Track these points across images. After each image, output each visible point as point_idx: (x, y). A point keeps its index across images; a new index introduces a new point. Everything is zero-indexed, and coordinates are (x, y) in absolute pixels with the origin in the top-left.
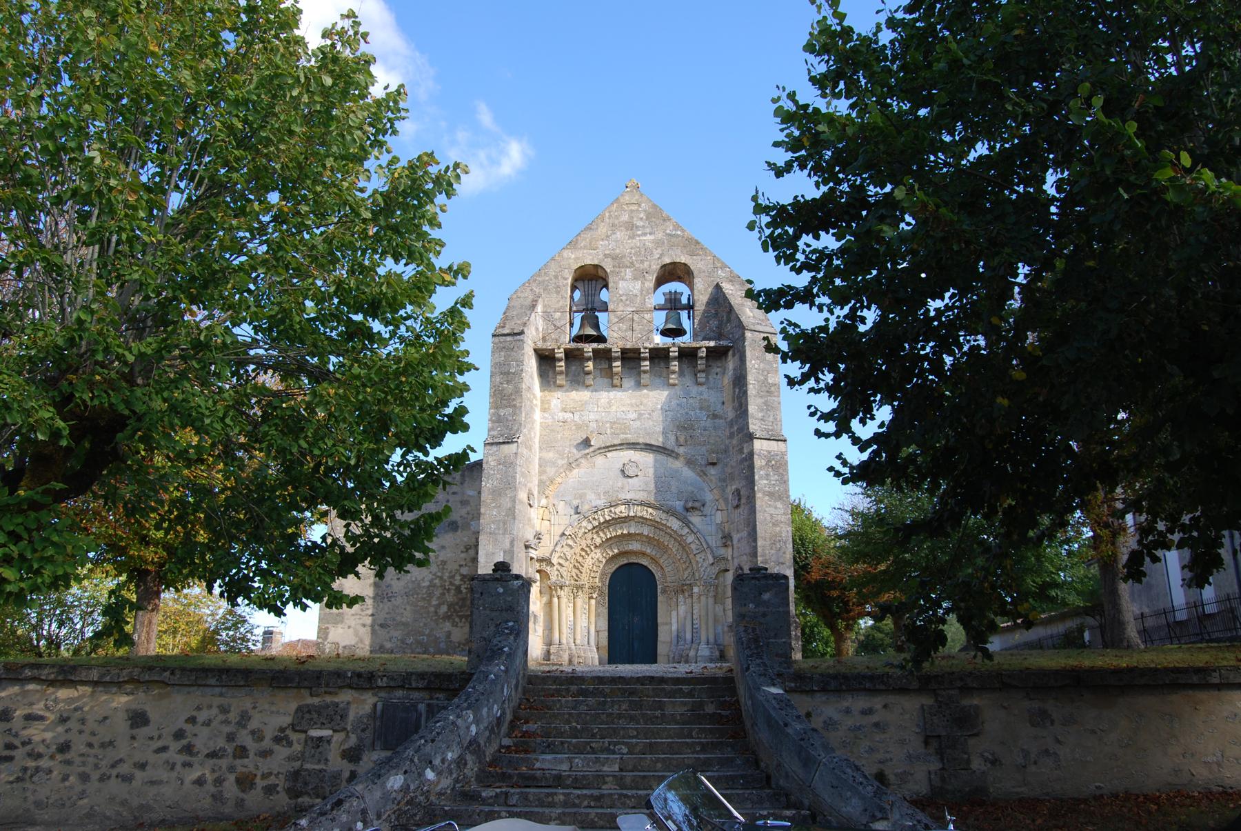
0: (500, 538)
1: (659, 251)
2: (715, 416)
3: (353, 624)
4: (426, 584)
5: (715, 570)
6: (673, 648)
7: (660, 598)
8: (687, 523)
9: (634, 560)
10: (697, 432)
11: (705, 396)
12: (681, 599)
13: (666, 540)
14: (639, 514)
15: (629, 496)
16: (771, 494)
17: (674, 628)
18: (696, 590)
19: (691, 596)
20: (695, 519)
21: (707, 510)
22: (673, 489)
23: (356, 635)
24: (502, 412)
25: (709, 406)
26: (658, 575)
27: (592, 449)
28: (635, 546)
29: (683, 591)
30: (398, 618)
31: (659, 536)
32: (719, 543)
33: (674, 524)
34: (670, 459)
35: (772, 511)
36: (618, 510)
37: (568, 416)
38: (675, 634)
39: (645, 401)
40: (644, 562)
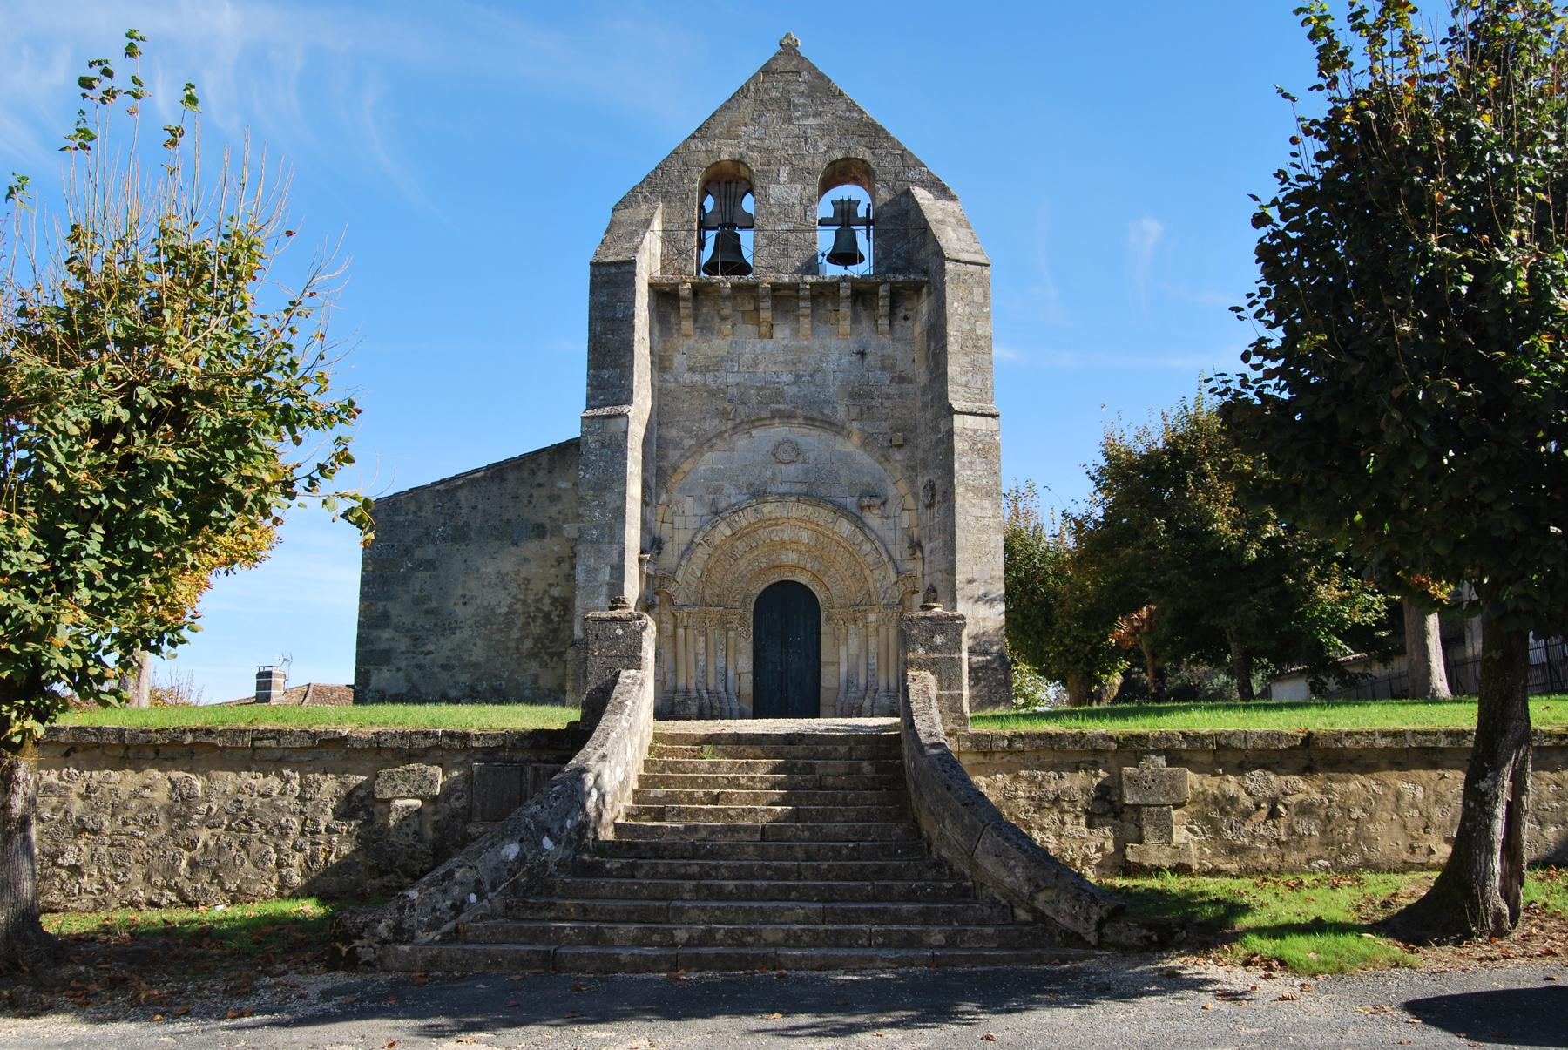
0: (605, 547)
1: (827, 140)
2: (902, 380)
3: (403, 665)
4: (504, 610)
6: (841, 696)
9: (788, 577)
10: (877, 402)
11: (889, 351)
16: (974, 490)
17: (843, 669)
18: (872, 617)
21: (890, 508)
23: (409, 680)
24: (605, 374)
25: (894, 366)
26: (821, 598)
30: (465, 656)
32: (906, 554)
33: (845, 527)
34: (839, 439)
35: (977, 512)
37: (697, 377)
38: (843, 676)
39: (804, 358)
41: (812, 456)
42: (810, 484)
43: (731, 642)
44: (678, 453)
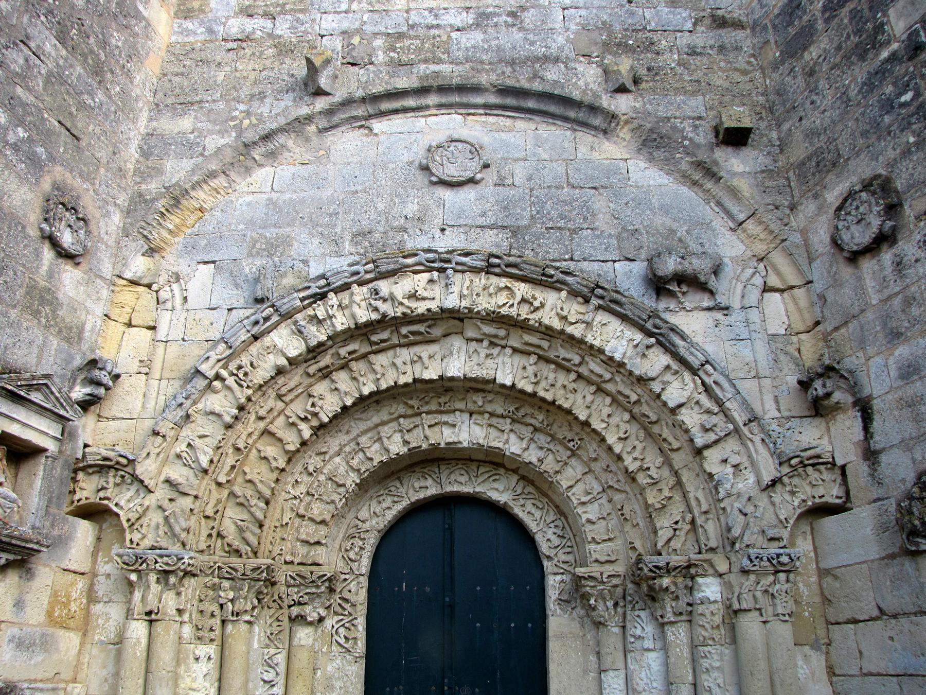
5: (787, 504)
7: (560, 623)
8: (661, 337)
9: (460, 483)
12: (643, 627)
13: (581, 401)
14: (484, 304)
15: (443, 244)
18: (710, 588)
19: (689, 615)
20: (691, 321)
21: (729, 289)
22: (602, 222)
26: (546, 538)
27: (321, 103)
28: (466, 432)
29: (653, 597)
31: (554, 386)
32: (792, 403)
33: (615, 338)
34: (585, 138)
36: (401, 287)
40: (499, 491)
41: (520, 173)
42: (515, 232)
43: (302, 660)
44: (187, 164)
